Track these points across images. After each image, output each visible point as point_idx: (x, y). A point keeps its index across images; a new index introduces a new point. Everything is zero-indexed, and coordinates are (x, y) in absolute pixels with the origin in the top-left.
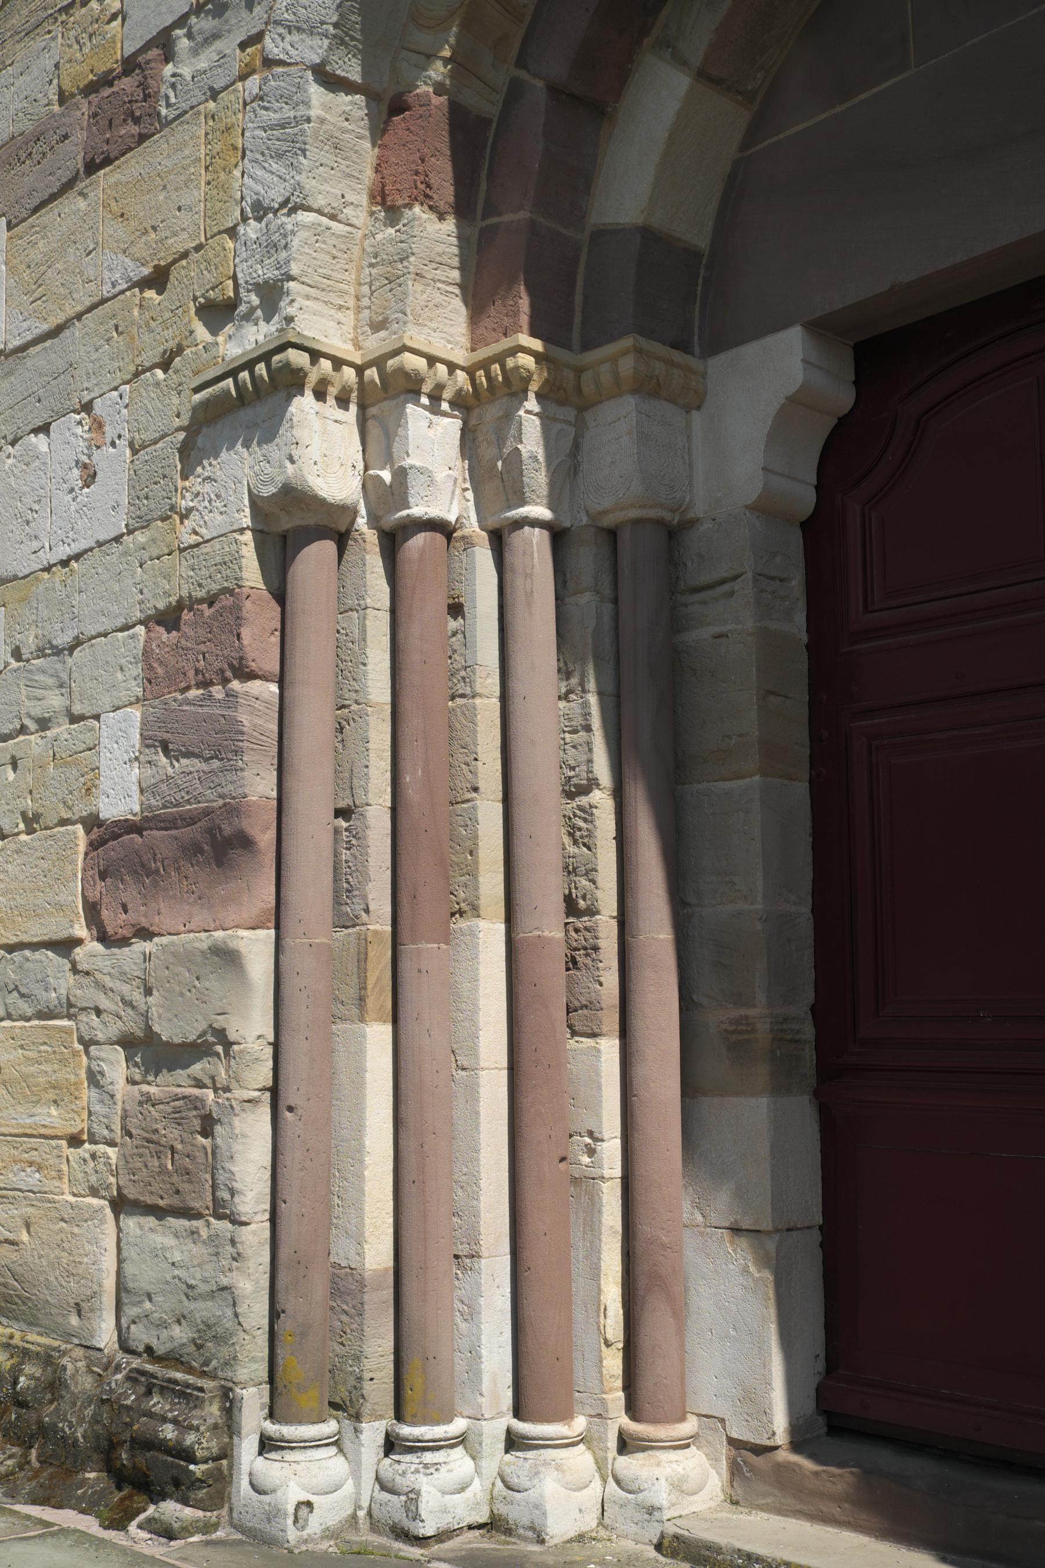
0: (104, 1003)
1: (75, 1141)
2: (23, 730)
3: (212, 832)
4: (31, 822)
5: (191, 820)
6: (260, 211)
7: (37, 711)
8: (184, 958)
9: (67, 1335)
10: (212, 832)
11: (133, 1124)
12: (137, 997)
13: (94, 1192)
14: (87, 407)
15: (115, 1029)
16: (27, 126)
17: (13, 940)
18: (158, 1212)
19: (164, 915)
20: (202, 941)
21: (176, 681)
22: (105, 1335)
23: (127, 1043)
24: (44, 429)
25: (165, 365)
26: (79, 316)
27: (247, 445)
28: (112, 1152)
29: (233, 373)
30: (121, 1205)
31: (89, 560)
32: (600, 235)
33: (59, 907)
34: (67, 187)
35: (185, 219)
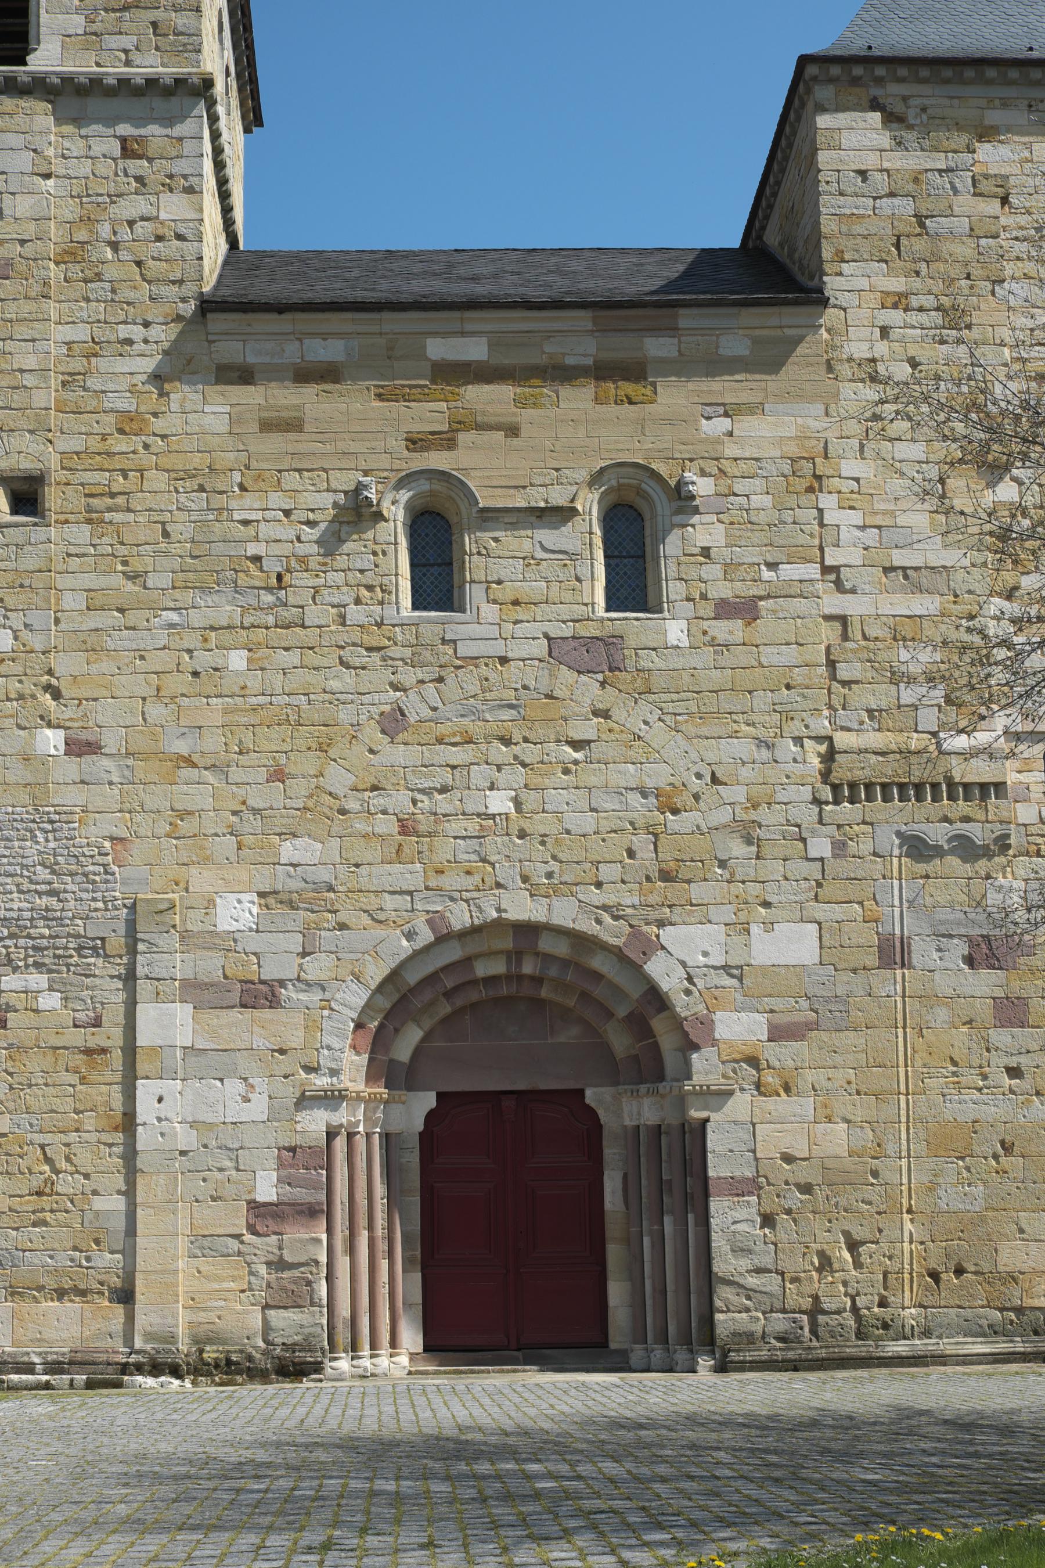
0: (258, 1252)
1: (243, 1291)
2: (209, 1170)
3: (310, 1209)
4: (214, 1199)
5: (302, 1204)
6: (329, 1048)
7: (219, 1165)
8: (301, 1241)
9: (245, 1345)
10: (310, 1209)
11: (273, 1285)
12: (276, 1251)
13: (253, 1305)
14: (245, 1079)
15: (263, 1259)
16: (207, 980)
17: (207, 1233)
18: (285, 1308)
19: (288, 1230)
20: (307, 1236)
21: (291, 1166)
22: (261, 1344)
23: (269, 1264)
24: (221, 1080)
25: (286, 1077)
26: (239, 1050)
27: (326, 1110)
28: (263, 1294)
29: (325, 1091)
30: (266, 1307)
31: (248, 1125)
32: (391, 1061)
33: (234, 1225)
34: (233, 1007)
35: (296, 1039)
